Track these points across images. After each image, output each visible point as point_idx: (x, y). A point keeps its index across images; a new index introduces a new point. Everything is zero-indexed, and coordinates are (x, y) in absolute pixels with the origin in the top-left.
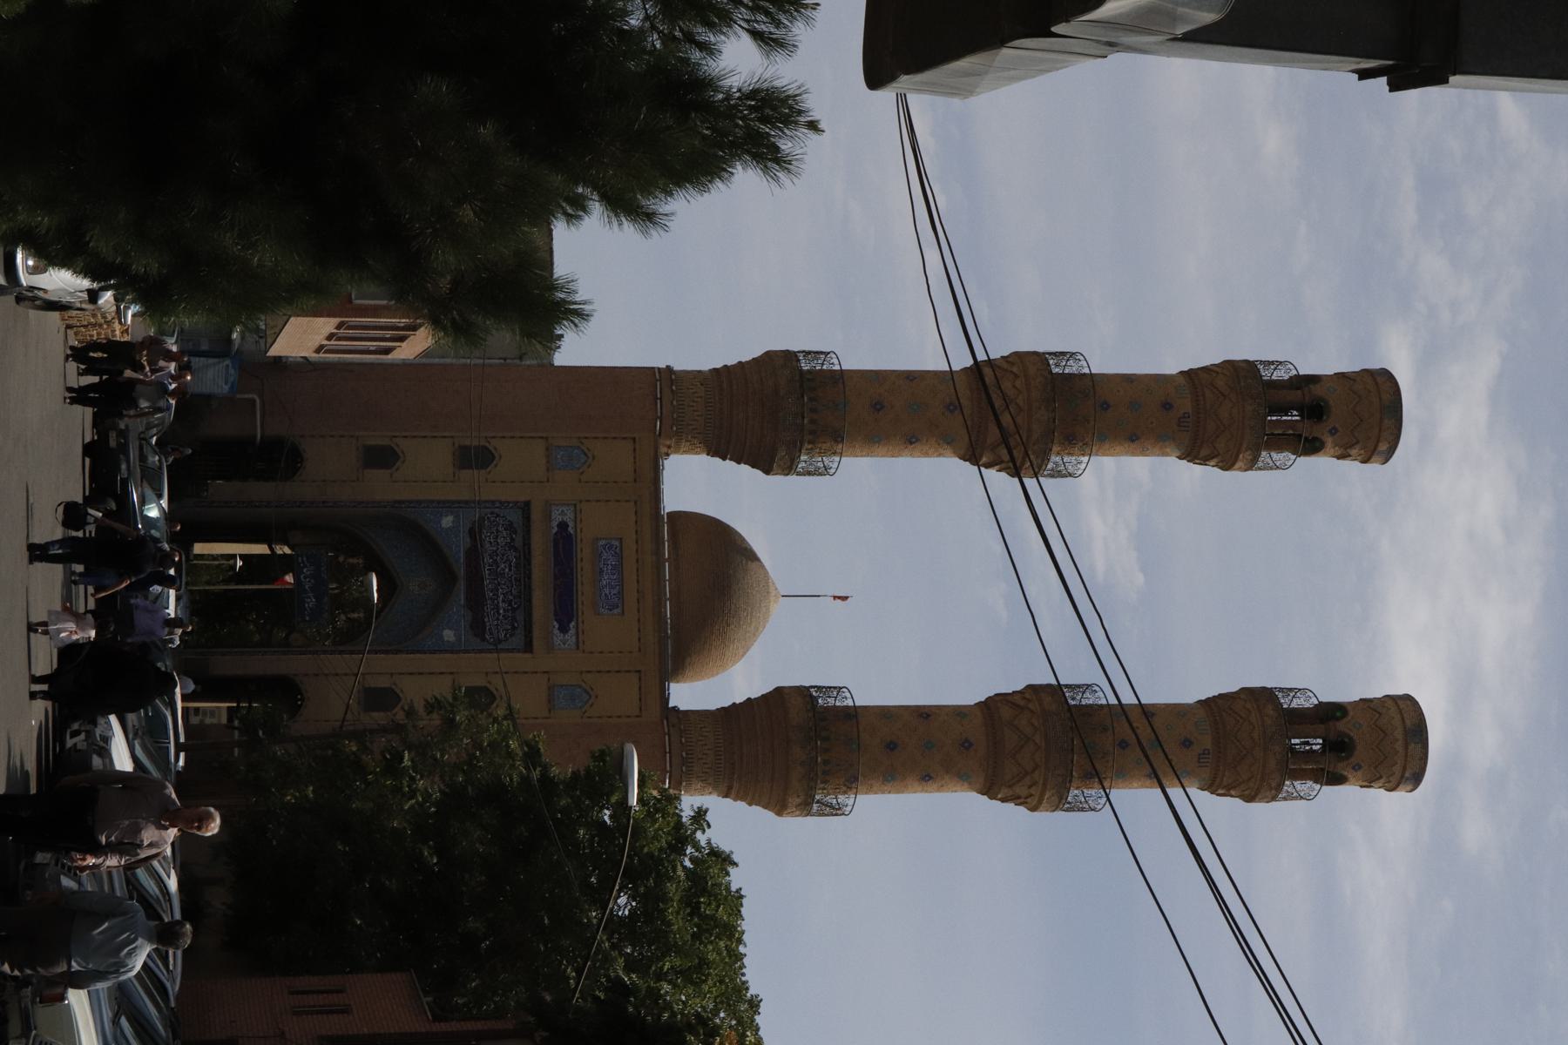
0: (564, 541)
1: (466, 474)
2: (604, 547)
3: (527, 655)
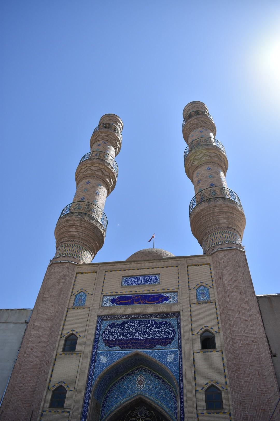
0: (121, 300)
1: (78, 348)
2: (126, 284)
3: (181, 314)
